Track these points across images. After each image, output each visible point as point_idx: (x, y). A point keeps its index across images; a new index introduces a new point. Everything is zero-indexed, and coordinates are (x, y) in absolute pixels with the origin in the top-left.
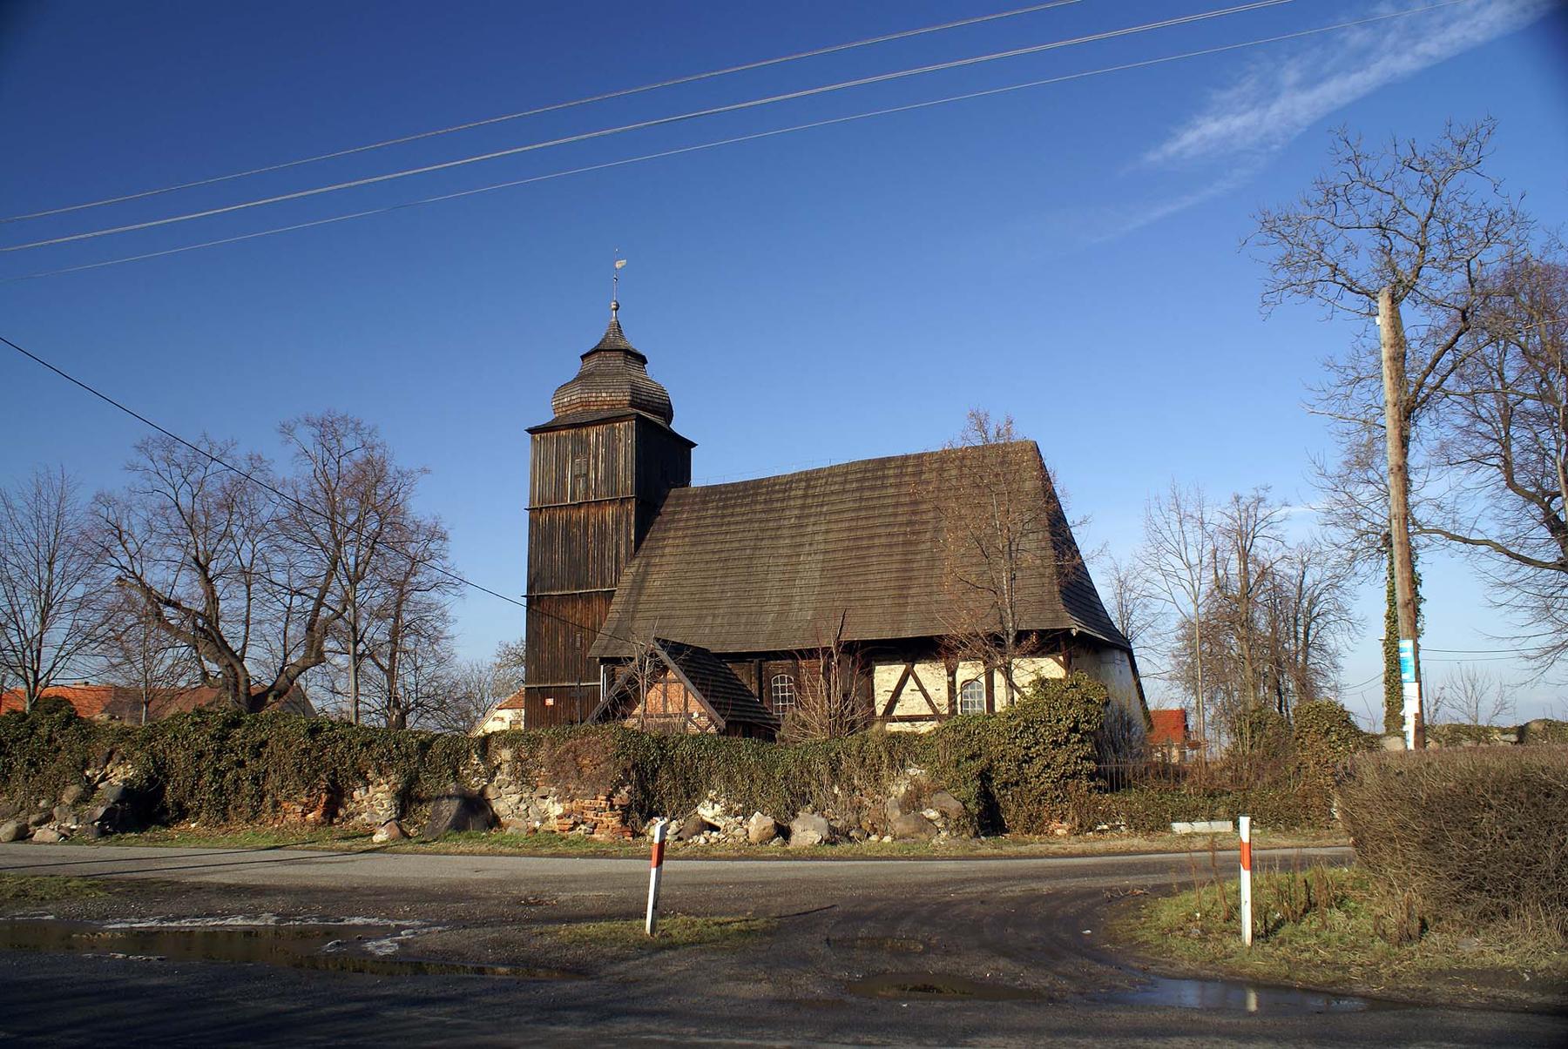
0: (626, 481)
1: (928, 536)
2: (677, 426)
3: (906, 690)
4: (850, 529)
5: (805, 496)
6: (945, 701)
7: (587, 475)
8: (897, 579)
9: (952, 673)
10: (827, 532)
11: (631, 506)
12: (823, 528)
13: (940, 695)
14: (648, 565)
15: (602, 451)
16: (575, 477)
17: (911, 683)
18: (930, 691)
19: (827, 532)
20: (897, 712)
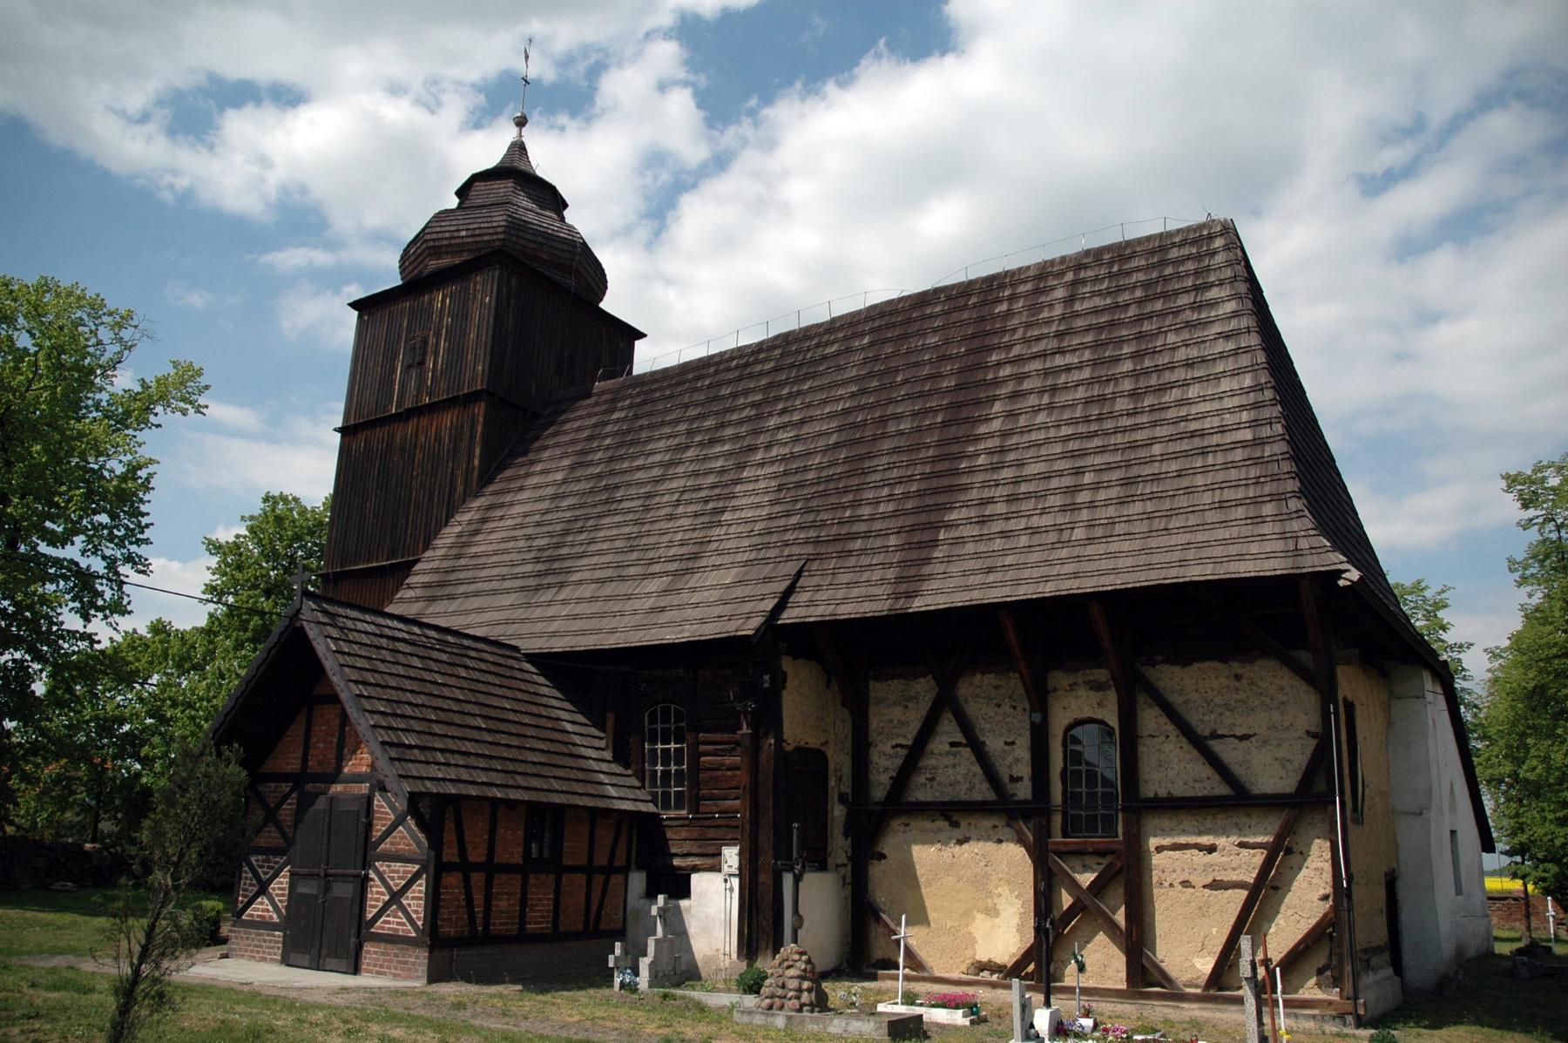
0: (476, 373)
1: (997, 407)
2: (610, 304)
3: (939, 744)
4: (846, 412)
5: (776, 370)
6: (1024, 770)
7: (422, 363)
8: (920, 494)
9: (1039, 699)
10: (802, 422)
11: (480, 409)
12: (796, 417)
13: (1016, 762)
14: (491, 507)
15: (447, 320)
16: (408, 368)
17: (949, 731)
18: (994, 744)
19: (802, 422)
20: (921, 792)
